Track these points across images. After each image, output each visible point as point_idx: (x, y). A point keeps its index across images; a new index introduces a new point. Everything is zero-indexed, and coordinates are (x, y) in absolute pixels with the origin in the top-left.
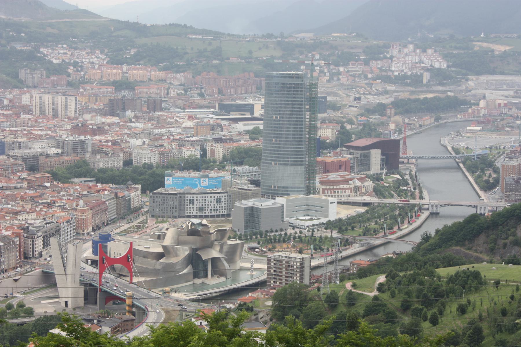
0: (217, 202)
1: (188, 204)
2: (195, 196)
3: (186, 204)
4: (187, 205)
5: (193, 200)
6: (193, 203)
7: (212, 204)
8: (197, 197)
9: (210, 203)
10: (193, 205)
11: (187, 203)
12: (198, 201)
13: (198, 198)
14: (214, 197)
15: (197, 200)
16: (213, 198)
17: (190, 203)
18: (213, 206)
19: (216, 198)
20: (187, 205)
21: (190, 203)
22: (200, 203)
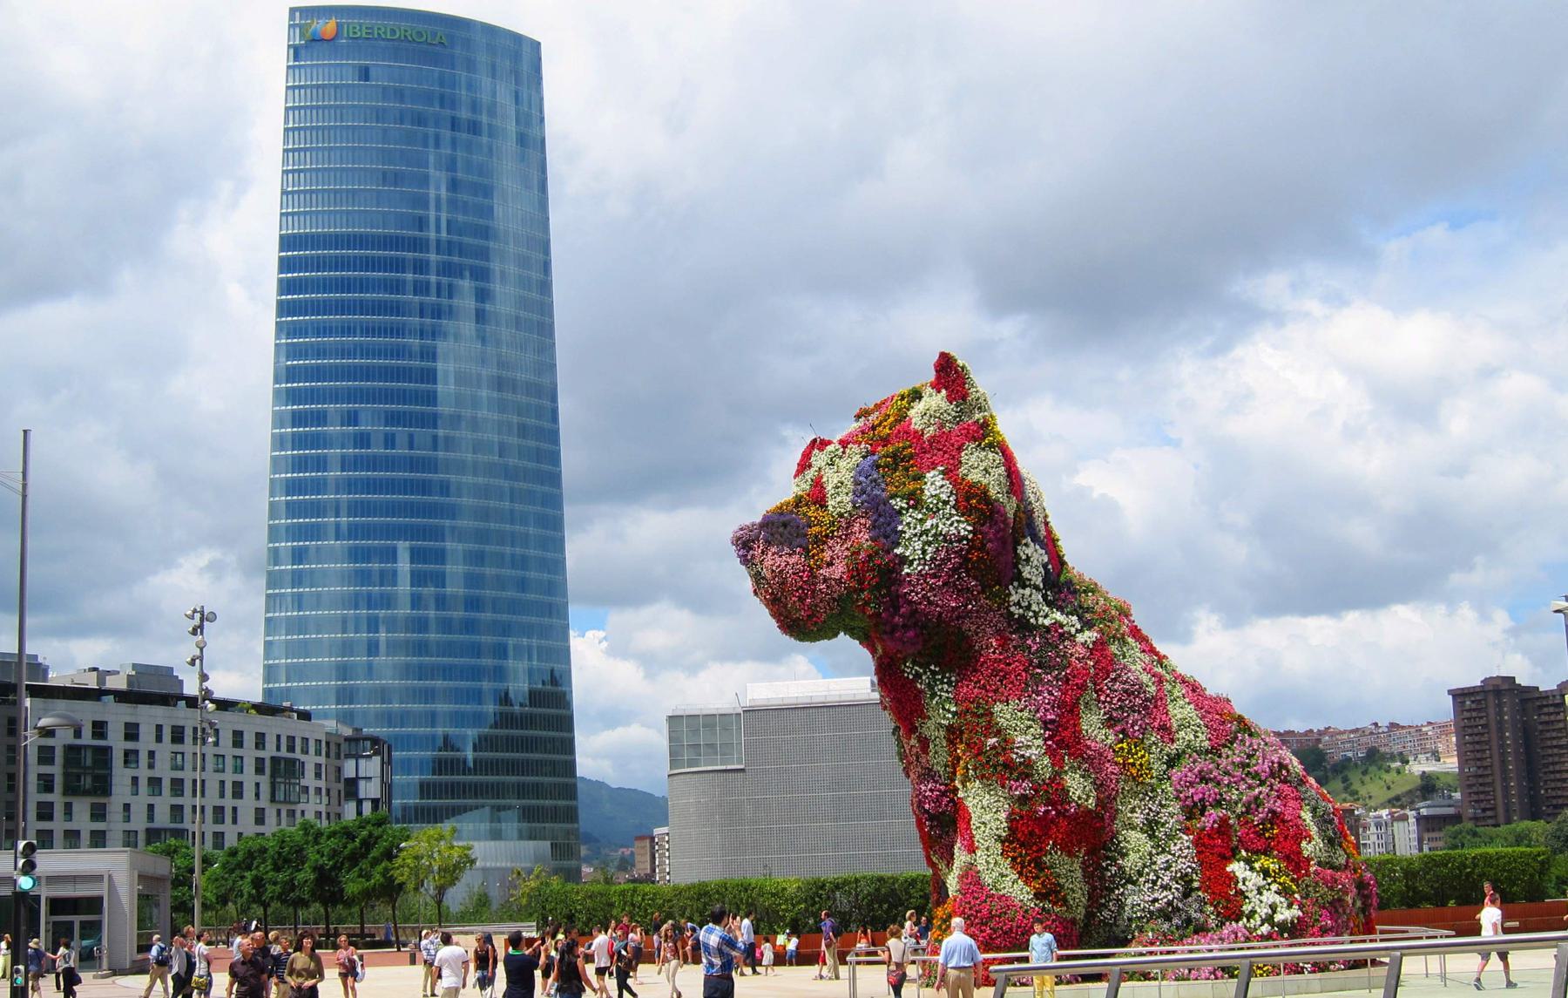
0: (273, 800)
1: (57, 798)
2: (117, 716)
3: (34, 797)
4: (45, 812)
5: (104, 754)
6: (103, 786)
7: (247, 805)
8: (132, 732)
9: (228, 802)
10: (99, 813)
11: (46, 784)
12: (144, 773)
13: (146, 741)
14: (260, 740)
15: (130, 757)
16: (249, 753)
17: (71, 789)
18: (247, 825)
19: (269, 752)
20: (45, 812)
21: (71, 789)
22: (155, 783)
